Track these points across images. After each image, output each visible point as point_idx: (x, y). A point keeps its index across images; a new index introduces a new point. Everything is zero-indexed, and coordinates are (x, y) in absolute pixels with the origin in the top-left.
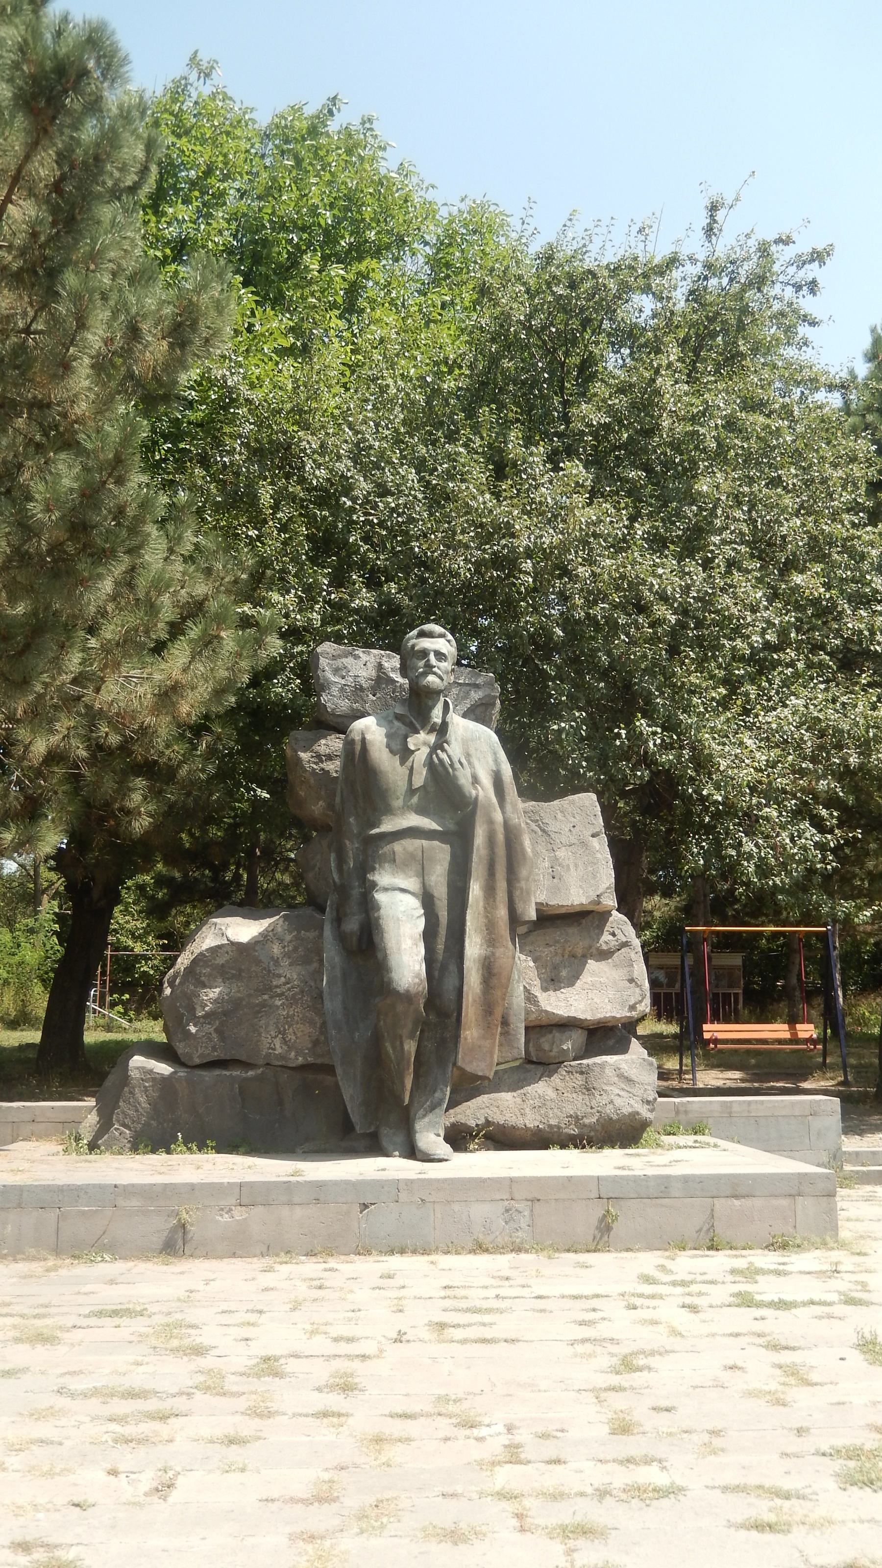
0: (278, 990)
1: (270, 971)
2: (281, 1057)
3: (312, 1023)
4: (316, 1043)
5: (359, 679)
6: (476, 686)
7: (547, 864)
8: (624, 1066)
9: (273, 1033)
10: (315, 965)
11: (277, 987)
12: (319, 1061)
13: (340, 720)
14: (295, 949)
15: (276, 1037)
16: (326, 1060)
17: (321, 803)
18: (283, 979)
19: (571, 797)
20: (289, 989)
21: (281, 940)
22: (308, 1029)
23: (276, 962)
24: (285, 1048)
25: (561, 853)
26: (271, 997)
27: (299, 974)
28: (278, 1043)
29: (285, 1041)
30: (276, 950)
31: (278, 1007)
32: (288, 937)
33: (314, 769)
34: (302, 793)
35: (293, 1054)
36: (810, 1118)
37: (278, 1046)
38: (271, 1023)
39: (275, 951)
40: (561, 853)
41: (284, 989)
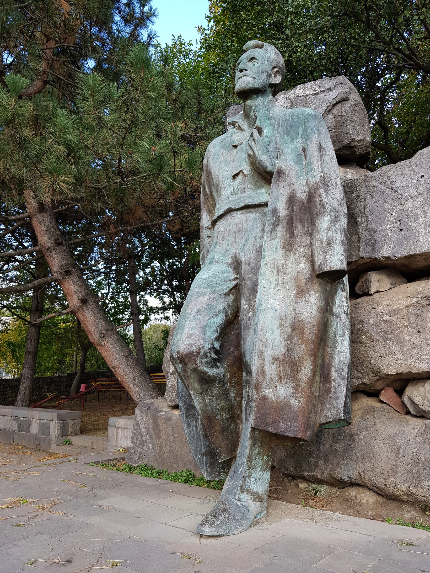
6: (330, 89)
7: (394, 219)
25: (410, 205)
40: (410, 205)
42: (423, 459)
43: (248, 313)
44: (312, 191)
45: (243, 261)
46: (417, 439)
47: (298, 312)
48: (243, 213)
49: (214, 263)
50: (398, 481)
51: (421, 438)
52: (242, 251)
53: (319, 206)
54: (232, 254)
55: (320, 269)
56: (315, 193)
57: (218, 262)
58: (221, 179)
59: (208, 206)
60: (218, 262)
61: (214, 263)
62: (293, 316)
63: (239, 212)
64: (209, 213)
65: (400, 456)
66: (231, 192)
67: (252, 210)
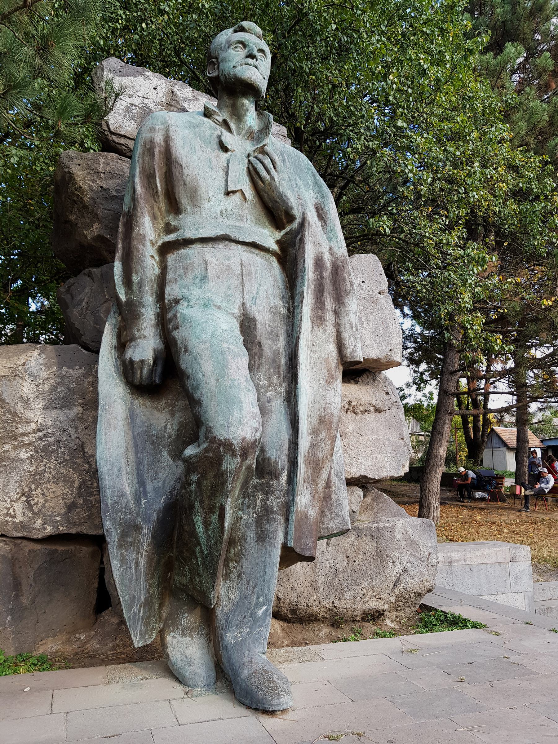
0: (26, 440)
1: (16, 414)
2: (22, 526)
3: (68, 482)
4: (71, 507)
5: (146, 101)
8: (410, 530)
9: (13, 495)
10: (78, 410)
11: (23, 435)
12: (73, 531)
13: (122, 141)
14: (53, 390)
15: (18, 499)
16: (84, 529)
17: (96, 225)
18: (33, 426)
19: (358, 256)
20: (40, 439)
21: (34, 377)
22: (60, 489)
23: (26, 402)
24: (30, 514)
26: (15, 448)
27: (56, 420)
28: (19, 507)
29: (29, 505)
30: (27, 388)
31: (23, 461)
32: (44, 374)
33: (90, 186)
34: (73, 218)
35: (39, 522)
36: (510, 563)
37: (19, 511)
38: (12, 482)
39: (25, 389)
41: (32, 438)
42: (341, 569)
43: (267, 391)
44: (339, 263)
45: (258, 318)
46: (330, 548)
47: (328, 402)
48: (246, 251)
49: (213, 307)
50: (321, 598)
51: (334, 548)
52: (254, 304)
53: (348, 282)
54: (238, 304)
55: (353, 357)
56: (343, 267)
57: (219, 308)
58: (202, 183)
59: (152, 208)
60: (219, 308)
61: (213, 307)
62: (323, 405)
63: (240, 246)
64: (152, 219)
65: (317, 570)
66: (221, 212)
67: (256, 251)
